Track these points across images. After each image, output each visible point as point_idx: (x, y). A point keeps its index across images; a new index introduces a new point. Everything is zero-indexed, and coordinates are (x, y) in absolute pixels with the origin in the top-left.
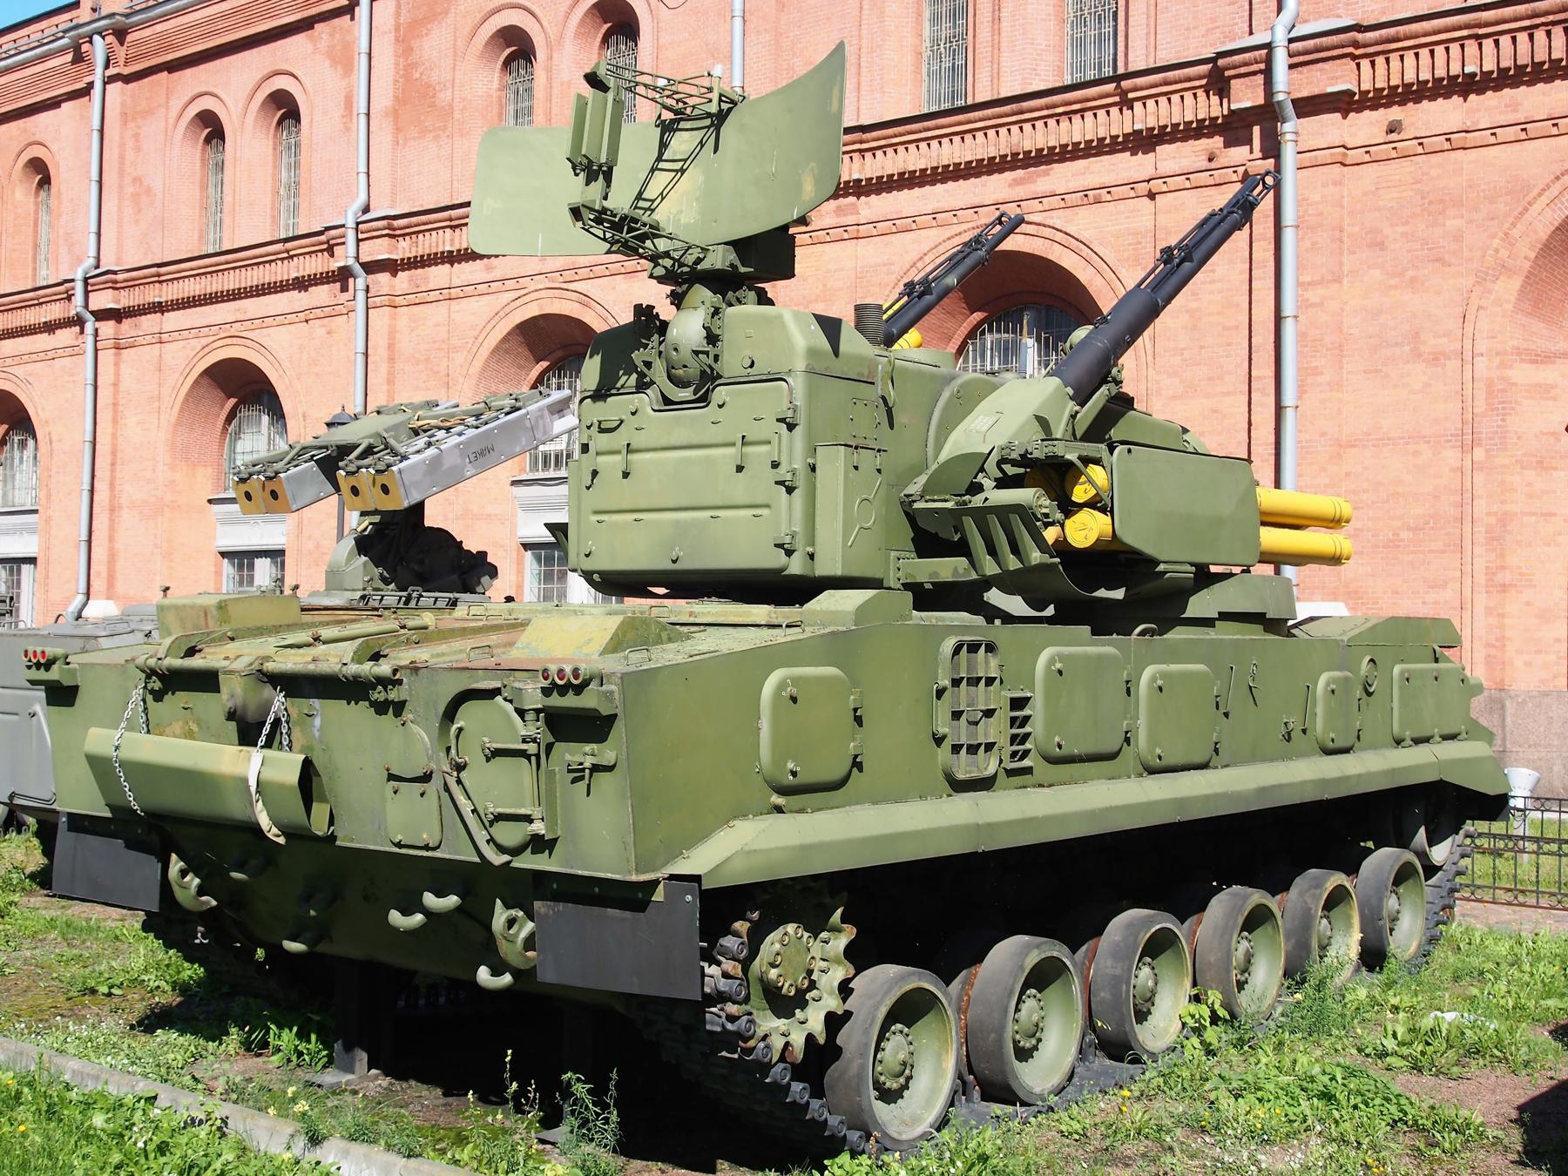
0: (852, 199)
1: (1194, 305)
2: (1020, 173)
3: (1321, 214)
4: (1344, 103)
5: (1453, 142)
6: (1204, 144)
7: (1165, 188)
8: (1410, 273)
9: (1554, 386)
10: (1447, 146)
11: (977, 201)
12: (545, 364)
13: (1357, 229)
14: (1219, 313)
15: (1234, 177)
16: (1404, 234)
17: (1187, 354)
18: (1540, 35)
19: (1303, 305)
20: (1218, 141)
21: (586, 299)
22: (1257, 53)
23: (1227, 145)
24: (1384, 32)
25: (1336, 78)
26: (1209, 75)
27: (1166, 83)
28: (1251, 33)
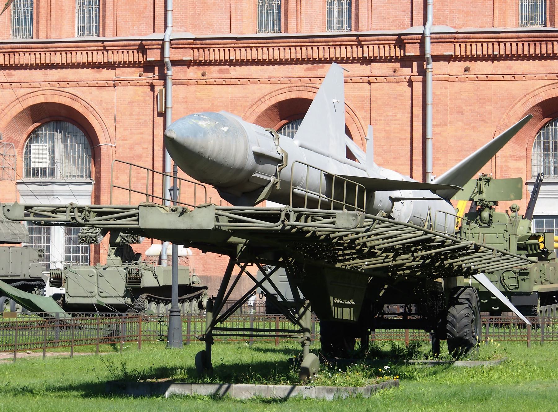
0: (227, 67)
1: (387, 128)
2: (310, 66)
3: (440, 99)
4: (449, 59)
5: (488, 78)
6: (392, 65)
7: (375, 81)
8: (473, 124)
9: (522, 169)
10: (486, 79)
11: (289, 75)
12: (37, 124)
13: (453, 106)
14: (398, 133)
15: (405, 80)
16: (470, 110)
17: (385, 148)
18: (520, 44)
19: (434, 133)
20: (398, 65)
21: (75, 97)
22: (417, 36)
23: (402, 67)
24: (465, 35)
25: (447, 50)
26: (396, 40)
27: (378, 40)
28: (412, 25)
